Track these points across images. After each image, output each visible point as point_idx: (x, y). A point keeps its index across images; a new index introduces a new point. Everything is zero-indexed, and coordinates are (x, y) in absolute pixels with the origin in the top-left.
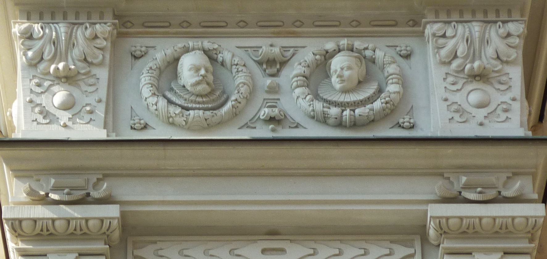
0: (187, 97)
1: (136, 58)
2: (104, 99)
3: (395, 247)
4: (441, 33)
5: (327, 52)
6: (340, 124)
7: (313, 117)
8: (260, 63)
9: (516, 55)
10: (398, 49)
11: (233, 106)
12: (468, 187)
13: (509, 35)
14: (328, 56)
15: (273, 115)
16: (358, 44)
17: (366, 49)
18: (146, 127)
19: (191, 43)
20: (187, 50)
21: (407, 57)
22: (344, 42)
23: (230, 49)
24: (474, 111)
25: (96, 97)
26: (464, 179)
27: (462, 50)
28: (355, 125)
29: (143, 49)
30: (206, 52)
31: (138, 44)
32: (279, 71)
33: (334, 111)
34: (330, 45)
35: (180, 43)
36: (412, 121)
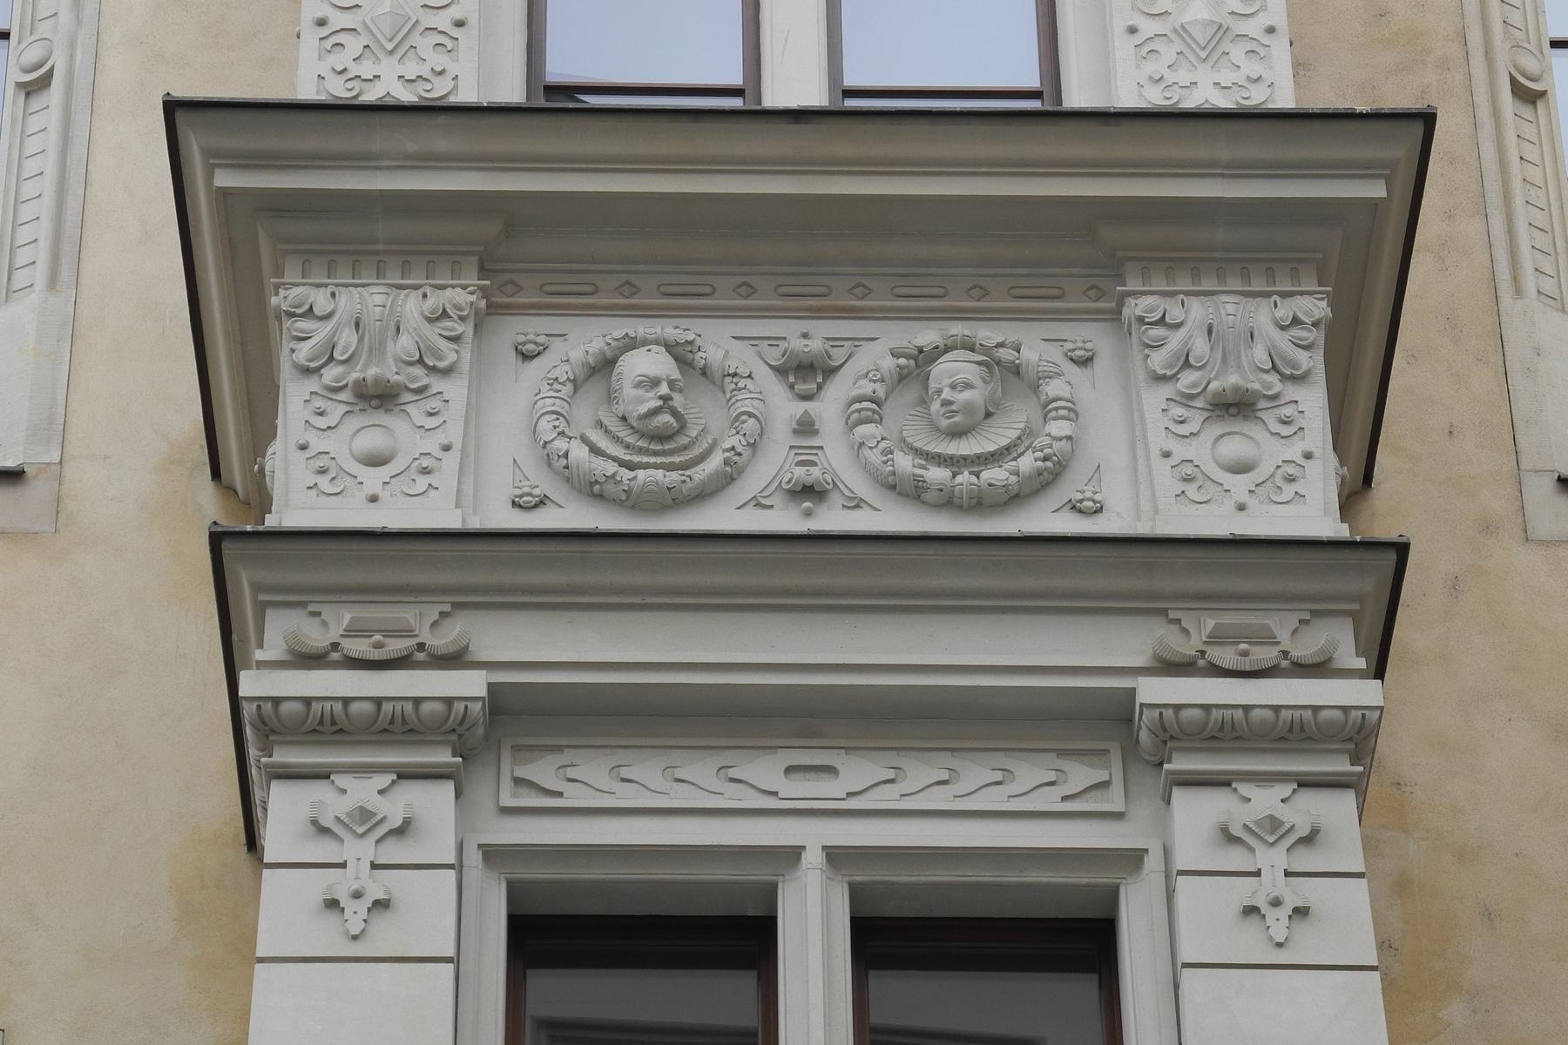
0: (630, 440)
1: (526, 357)
2: (457, 446)
3: (1068, 765)
4: (1157, 316)
5: (921, 351)
6: (949, 502)
7: (893, 487)
8: (781, 371)
9: (1312, 361)
10: (1069, 346)
11: (726, 462)
12: (1216, 639)
13: (1296, 321)
14: (925, 358)
15: (808, 481)
16: (988, 334)
17: (1001, 345)
18: (542, 502)
19: (641, 328)
20: (631, 344)
21: (1085, 362)
22: (958, 329)
23: (719, 342)
24: (1228, 479)
25: (440, 438)
26: (1210, 623)
27: (1200, 346)
28: (980, 504)
29: (541, 339)
30: (670, 347)
31: (532, 328)
32: (820, 388)
33: (936, 474)
34: (928, 335)
35: (620, 328)
36: (1098, 497)
